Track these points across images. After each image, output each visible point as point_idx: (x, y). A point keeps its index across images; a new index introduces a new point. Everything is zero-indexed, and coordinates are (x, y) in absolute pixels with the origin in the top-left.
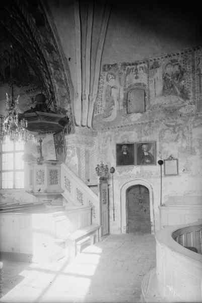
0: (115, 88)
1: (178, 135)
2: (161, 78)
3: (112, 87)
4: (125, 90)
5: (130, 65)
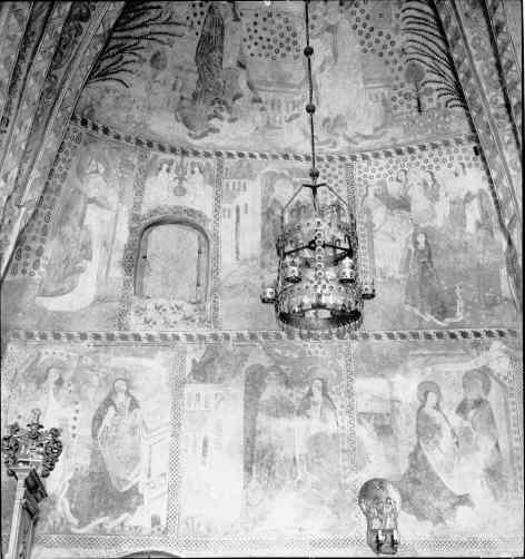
1: (310, 394)
2: (259, 210)
4: (135, 218)
5: (162, 149)
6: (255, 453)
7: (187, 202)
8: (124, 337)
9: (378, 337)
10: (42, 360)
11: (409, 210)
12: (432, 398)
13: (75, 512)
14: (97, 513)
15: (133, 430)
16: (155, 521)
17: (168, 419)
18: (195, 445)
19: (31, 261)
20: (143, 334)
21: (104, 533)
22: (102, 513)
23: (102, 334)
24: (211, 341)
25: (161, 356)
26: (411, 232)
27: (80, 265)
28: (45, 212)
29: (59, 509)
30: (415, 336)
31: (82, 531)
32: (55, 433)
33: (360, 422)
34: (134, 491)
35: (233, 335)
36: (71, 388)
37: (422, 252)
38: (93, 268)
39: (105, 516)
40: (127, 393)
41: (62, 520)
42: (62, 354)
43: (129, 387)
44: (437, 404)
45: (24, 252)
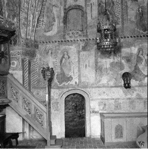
0: (56, 7)
2: (97, 4)
3: (54, 6)
4: (65, 9)
6: (98, 67)
7: (78, 3)
8: (65, 41)
9: (128, 37)
10: (47, 48)
11: (137, 1)
12: (141, 52)
13: (58, 82)
14: (63, 81)
15: (69, 63)
16: (76, 83)
17: (77, 60)
18: (84, 66)
19: (41, 24)
20: (69, 40)
21: (65, 86)
22: (64, 82)
23: (60, 41)
24: (86, 41)
25: (74, 45)
26: (138, 7)
27: (52, 23)
28: (43, 11)
29: (55, 81)
30: (138, 36)
31: (60, 86)
32: (52, 69)
33: (123, 59)
34: (71, 77)
35: (91, 39)
36: (54, 54)
37: (141, 13)
38: (56, 23)
39: (65, 82)
40: (67, 55)
41: (56, 83)
42: (51, 46)
43: (67, 54)
44: (142, 54)
45: (39, 22)
